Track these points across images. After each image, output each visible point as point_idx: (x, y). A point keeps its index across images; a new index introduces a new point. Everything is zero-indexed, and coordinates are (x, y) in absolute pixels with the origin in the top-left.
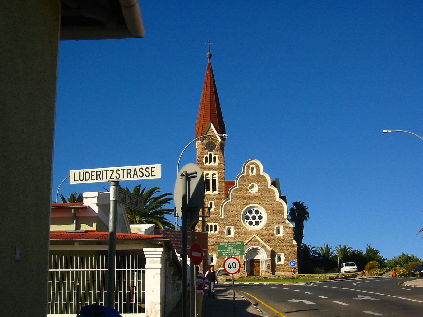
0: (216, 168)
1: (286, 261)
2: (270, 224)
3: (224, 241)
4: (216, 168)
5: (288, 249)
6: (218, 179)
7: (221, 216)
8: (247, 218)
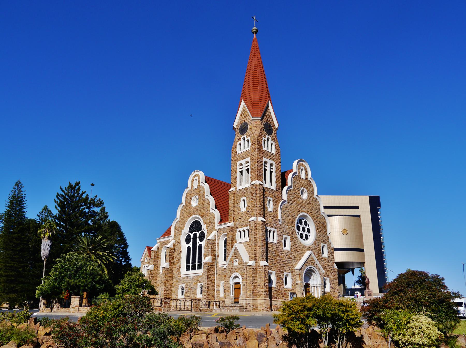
0: (273, 158)
1: (331, 288)
2: (318, 241)
3: (282, 254)
4: (273, 158)
5: (332, 274)
6: (276, 172)
7: (280, 221)
8: (298, 228)
